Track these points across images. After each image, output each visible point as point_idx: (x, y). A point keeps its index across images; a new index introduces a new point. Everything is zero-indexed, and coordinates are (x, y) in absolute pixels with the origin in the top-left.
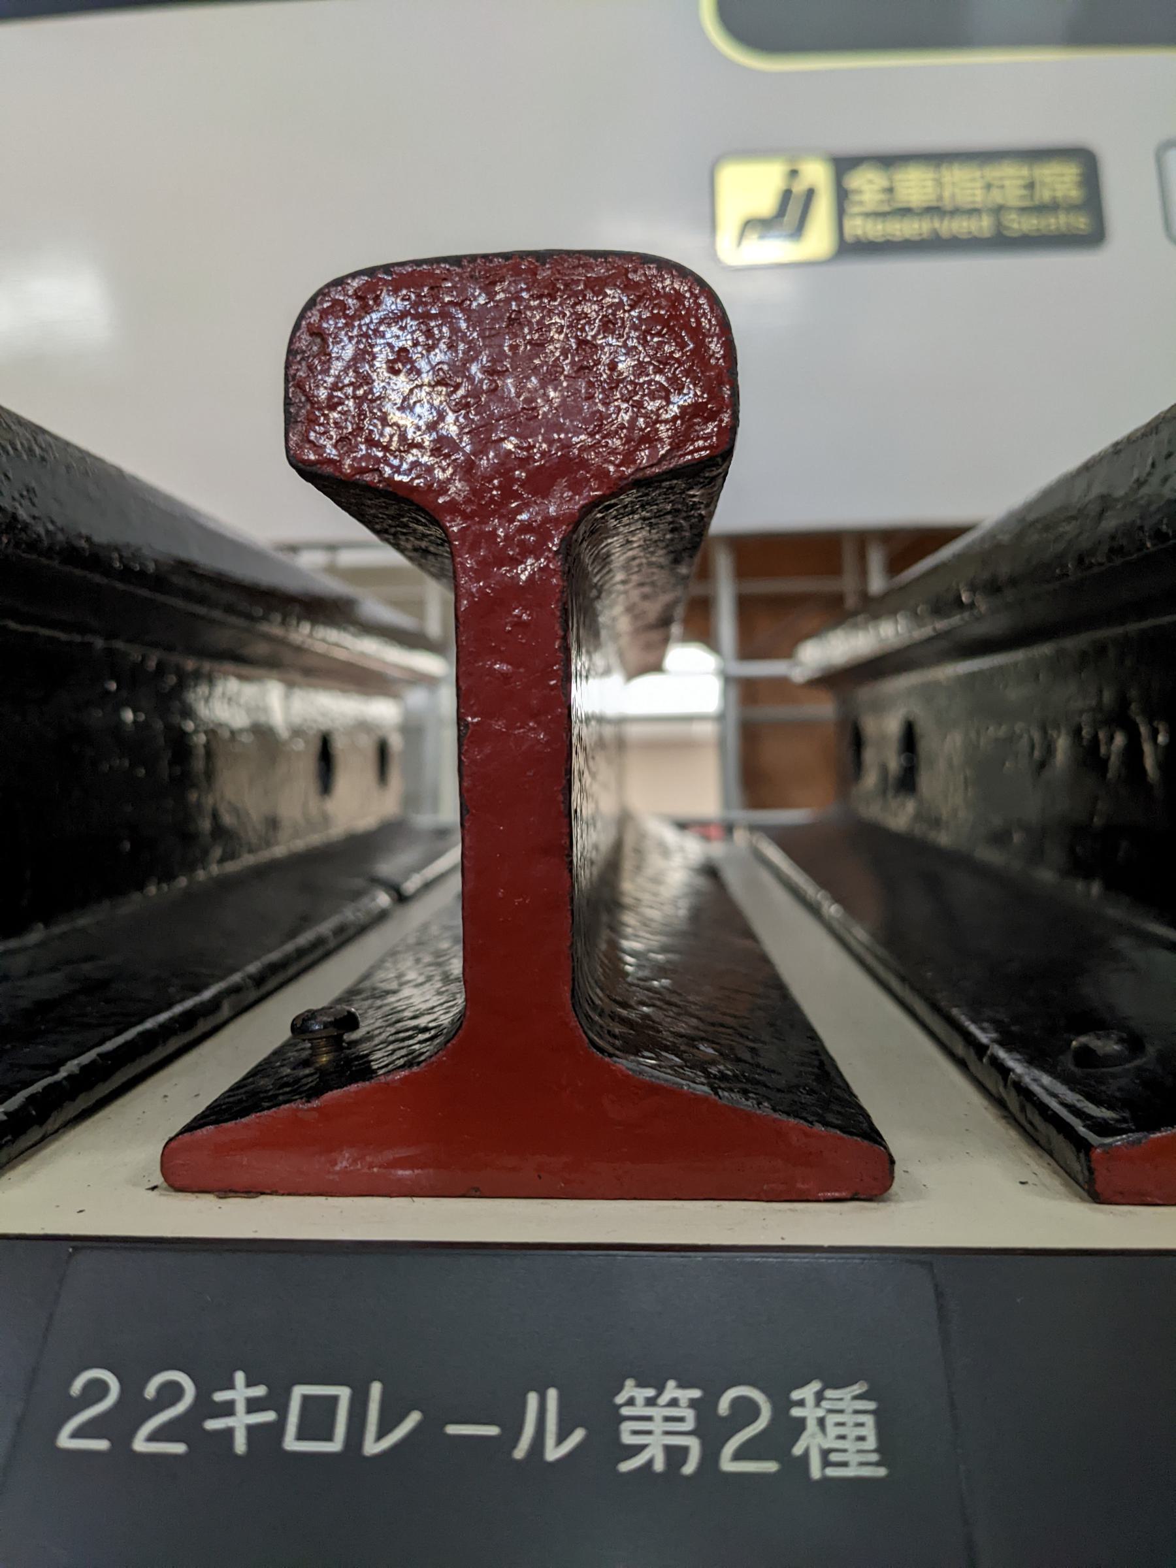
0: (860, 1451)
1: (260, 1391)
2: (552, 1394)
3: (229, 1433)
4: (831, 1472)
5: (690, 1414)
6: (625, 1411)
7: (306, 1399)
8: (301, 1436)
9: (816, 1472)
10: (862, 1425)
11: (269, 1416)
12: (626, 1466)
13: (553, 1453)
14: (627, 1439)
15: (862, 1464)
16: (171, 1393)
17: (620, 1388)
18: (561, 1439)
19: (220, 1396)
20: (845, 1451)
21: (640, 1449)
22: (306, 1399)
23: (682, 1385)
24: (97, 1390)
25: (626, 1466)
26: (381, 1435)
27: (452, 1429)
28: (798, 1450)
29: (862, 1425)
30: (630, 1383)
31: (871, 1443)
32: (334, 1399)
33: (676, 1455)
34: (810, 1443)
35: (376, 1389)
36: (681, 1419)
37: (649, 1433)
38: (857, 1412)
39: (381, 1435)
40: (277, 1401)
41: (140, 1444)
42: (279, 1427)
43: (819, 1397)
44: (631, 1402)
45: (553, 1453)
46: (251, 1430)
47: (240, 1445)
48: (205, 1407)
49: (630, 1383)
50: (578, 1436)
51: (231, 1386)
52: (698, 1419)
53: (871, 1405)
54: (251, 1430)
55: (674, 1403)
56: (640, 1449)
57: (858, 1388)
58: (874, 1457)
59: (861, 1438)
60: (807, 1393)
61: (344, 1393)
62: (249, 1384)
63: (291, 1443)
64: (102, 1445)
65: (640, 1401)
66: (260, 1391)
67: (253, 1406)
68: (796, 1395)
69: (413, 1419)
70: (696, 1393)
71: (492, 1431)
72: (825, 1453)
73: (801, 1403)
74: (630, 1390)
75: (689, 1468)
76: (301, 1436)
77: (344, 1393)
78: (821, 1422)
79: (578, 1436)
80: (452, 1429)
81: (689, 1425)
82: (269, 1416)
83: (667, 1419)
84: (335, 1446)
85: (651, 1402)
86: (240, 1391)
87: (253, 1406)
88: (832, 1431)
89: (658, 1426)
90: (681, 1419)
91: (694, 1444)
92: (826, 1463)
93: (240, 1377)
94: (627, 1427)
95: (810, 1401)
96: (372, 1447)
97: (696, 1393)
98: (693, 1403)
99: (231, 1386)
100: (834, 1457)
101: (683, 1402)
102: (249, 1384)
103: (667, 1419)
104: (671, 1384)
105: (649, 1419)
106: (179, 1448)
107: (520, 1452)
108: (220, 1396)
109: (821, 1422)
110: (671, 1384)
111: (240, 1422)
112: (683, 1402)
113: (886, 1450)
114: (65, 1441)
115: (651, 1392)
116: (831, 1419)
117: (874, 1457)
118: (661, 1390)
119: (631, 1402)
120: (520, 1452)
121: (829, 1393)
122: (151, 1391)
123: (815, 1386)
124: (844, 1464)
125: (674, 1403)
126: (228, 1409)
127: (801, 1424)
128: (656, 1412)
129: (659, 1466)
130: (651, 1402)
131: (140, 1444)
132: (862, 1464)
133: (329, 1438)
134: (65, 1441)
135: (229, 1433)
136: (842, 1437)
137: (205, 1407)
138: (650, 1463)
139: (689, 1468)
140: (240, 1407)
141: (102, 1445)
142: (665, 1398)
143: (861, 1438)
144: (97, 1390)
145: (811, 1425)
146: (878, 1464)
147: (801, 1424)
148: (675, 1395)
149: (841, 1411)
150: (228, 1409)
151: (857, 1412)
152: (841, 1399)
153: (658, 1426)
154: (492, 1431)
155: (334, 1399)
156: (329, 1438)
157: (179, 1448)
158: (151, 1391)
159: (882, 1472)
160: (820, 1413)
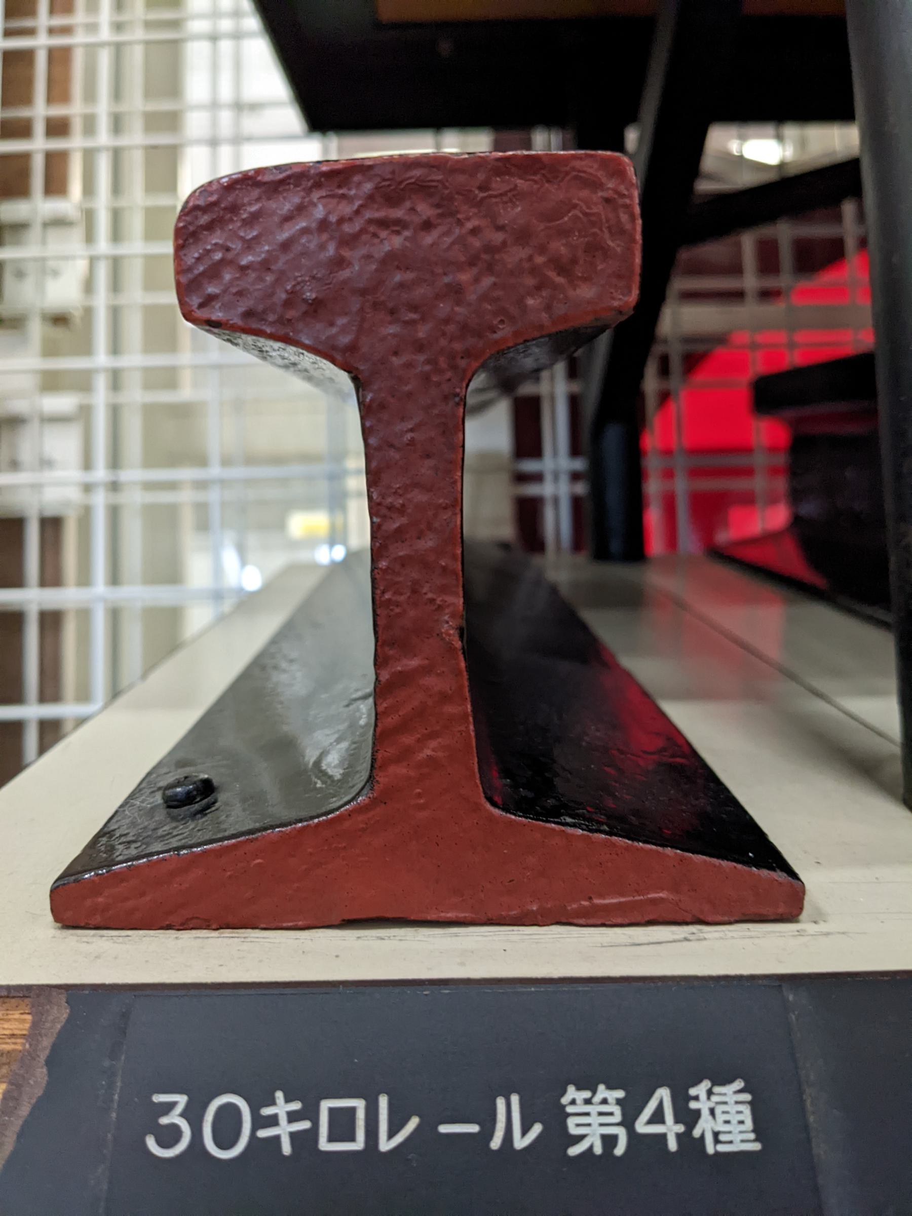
0: (741, 1132)
1: (296, 1106)
2: (515, 1099)
3: (277, 1138)
4: (721, 1148)
5: (617, 1110)
6: (570, 1109)
7: (332, 1111)
8: (331, 1139)
9: (710, 1149)
11: (305, 1125)
12: (574, 1151)
13: (520, 1143)
14: (573, 1130)
15: (743, 1141)
17: (564, 1092)
18: (524, 1132)
19: (267, 1111)
20: (730, 1132)
21: (582, 1137)
23: (610, 1087)
25: (574, 1151)
26: (391, 1135)
27: (444, 1129)
28: (697, 1133)
30: (571, 1090)
31: (749, 1125)
32: (353, 1110)
33: (609, 1141)
34: (704, 1126)
35: (383, 1102)
36: (611, 1114)
37: (589, 1125)
38: (737, 1103)
39: (391, 1135)
40: (310, 1112)
42: (314, 1132)
43: (710, 1093)
44: (573, 1102)
45: (520, 1143)
46: (293, 1136)
47: (286, 1148)
49: (571, 1090)
50: (537, 1129)
51: (273, 1103)
52: (624, 1114)
53: (747, 1097)
54: (293, 1136)
55: (605, 1101)
56: (582, 1137)
57: (739, 1084)
58: (752, 1136)
59: (741, 1122)
60: (700, 1090)
61: (359, 1105)
62: (287, 1100)
63: (324, 1145)
65: (578, 1101)
66: (296, 1106)
67: (293, 1117)
68: (693, 1092)
69: (413, 1123)
70: (620, 1094)
71: (474, 1128)
72: (716, 1135)
73: (696, 1098)
74: (572, 1092)
75: (620, 1150)
76: (331, 1139)
77: (359, 1105)
78: (712, 1112)
79: (537, 1129)
80: (444, 1129)
81: (617, 1118)
82: (305, 1125)
83: (601, 1114)
84: (359, 1145)
85: (588, 1102)
86: (281, 1107)
87: (293, 1117)
88: (721, 1118)
89: (594, 1120)
90: (611, 1114)
91: (621, 1133)
92: (717, 1141)
93: (279, 1095)
94: (571, 1122)
95: (703, 1096)
96: (385, 1145)
97: (620, 1094)
98: (619, 1102)
99: (273, 1103)
100: (722, 1137)
101: (610, 1100)
102: (287, 1100)
103: (601, 1114)
104: (601, 1087)
105: (587, 1114)
107: (496, 1143)
108: (267, 1111)
109: (712, 1112)
110: (601, 1087)
111: (284, 1130)
113: (759, 1131)
115: (587, 1094)
116: (719, 1110)
118: (594, 1092)
119: (573, 1102)
120: (496, 1143)
121: (717, 1089)
123: (705, 1085)
124: (731, 1142)
125: (605, 1101)
126: (273, 1121)
127: (697, 1114)
128: (592, 1109)
129: (598, 1150)
130: (588, 1102)
132: (743, 1141)
133: (352, 1138)
135: (277, 1138)
136: (727, 1122)
138: (591, 1148)
139: (620, 1150)
140: (283, 1119)
143: (741, 1122)
145: (705, 1113)
146: (755, 1140)
147: (697, 1114)
149: (725, 1103)
150: (273, 1121)
151: (737, 1103)
152: (725, 1094)
153: (594, 1120)
154: (474, 1128)
155: (353, 1110)
156: (352, 1138)
159: (757, 1146)
160: (711, 1105)
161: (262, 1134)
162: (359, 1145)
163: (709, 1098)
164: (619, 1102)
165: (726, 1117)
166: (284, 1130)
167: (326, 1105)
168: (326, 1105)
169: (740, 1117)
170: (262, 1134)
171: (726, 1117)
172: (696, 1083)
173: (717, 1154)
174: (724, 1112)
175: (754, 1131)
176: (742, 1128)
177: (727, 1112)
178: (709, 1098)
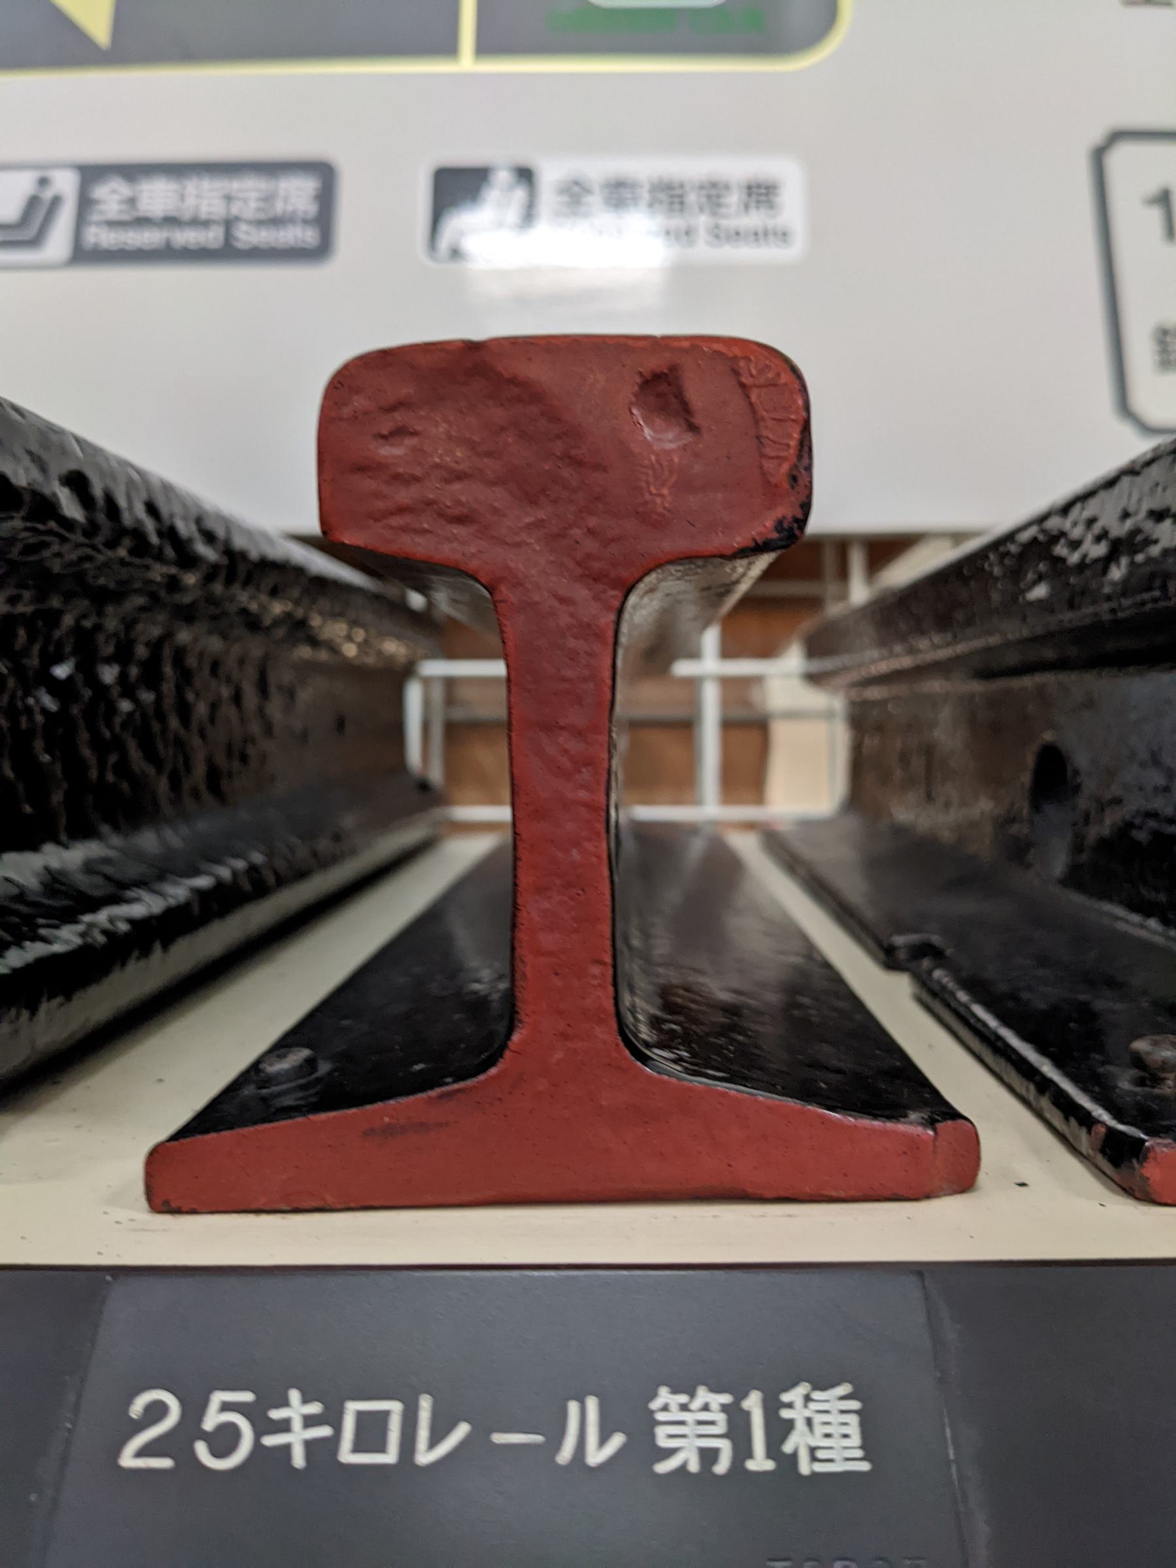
1: (315, 1408)
3: (287, 1449)
4: (819, 1468)
8: (357, 1448)
11: (325, 1431)
19: (276, 1414)
31: (856, 1440)
32: (386, 1414)
38: (843, 1412)
40: (333, 1417)
42: (334, 1442)
43: (808, 1399)
46: (309, 1445)
47: (298, 1459)
51: (285, 1403)
54: (309, 1445)
57: (844, 1389)
58: (859, 1453)
59: (846, 1436)
60: (794, 1395)
62: (305, 1400)
63: (347, 1455)
66: (315, 1408)
67: (310, 1421)
68: (786, 1397)
73: (790, 1405)
76: (357, 1448)
78: (809, 1422)
82: (325, 1431)
84: (390, 1457)
86: (296, 1408)
87: (310, 1421)
88: (819, 1430)
92: (814, 1459)
93: (294, 1396)
99: (285, 1403)
102: (305, 1400)
108: (276, 1414)
109: (809, 1422)
111: (296, 1439)
113: (869, 1447)
116: (818, 1419)
121: (816, 1395)
123: (802, 1389)
126: (284, 1426)
135: (287, 1449)
136: (828, 1436)
140: (297, 1424)
143: (846, 1436)
145: (800, 1425)
149: (827, 1412)
150: (284, 1426)
151: (843, 1412)
159: (865, 1466)
160: (807, 1413)
161: (270, 1441)
162: (390, 1457)
163: (806, 1406)
165: (828, 1429)
166: (296, 1439)
167: (353, 1407)
169: (845, 1430)
170: (270, 1441)
173: (815, 1475)
175: (863, 1447)
176: (846, 1442)
178: (806, 1406)
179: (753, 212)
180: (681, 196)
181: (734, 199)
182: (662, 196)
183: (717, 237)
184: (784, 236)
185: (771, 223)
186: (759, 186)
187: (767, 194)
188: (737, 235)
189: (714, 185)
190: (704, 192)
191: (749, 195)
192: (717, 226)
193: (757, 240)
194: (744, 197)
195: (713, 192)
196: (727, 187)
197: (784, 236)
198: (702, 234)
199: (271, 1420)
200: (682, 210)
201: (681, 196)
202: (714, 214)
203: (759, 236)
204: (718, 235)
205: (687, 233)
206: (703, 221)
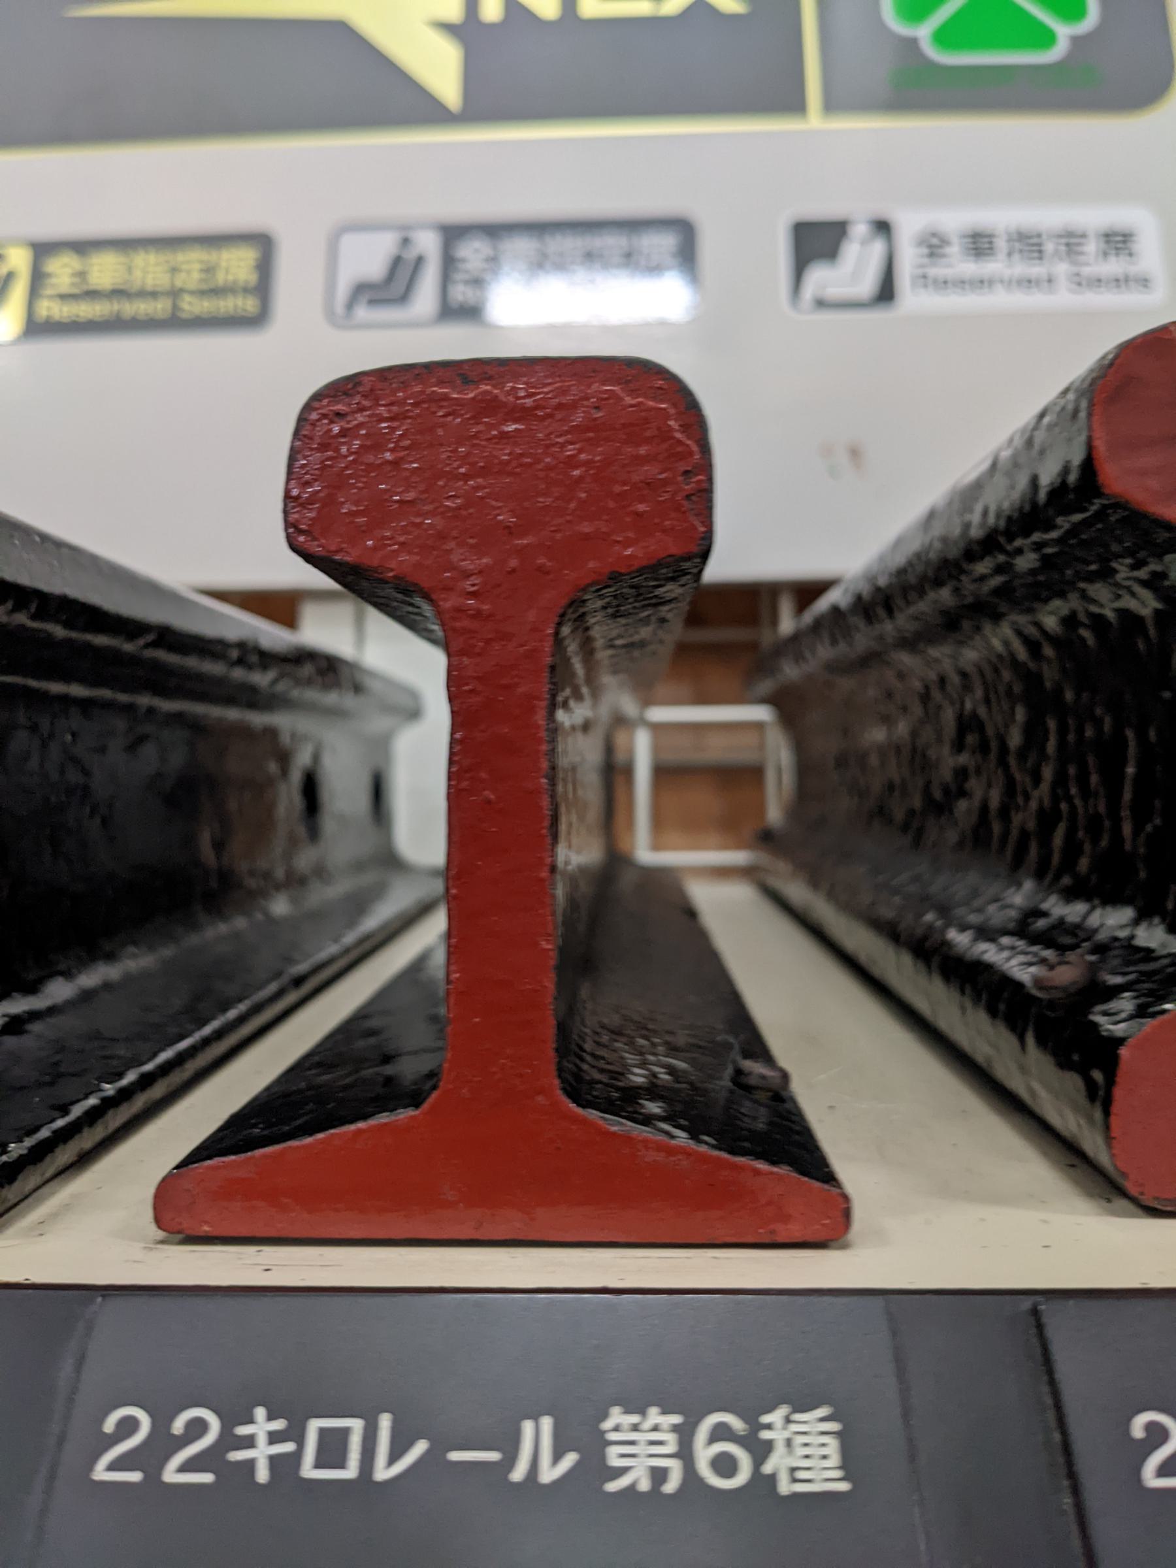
1: (279, 1425)
2: (547, 1423)
3: (250, 1464)
6: (613, 1436)
7: (323, 1432)
8: (318, 1465)
9: (785, 1487)
10: (823, 1445)
11: (289, 1447)
14: (615, 1462)
16: (197, 1428)
19: (243, 1430)
21: (624, 1471)
22: (323, 1432)
23: (665, 1412)
24: (128, 1427)
27: (455, 1456)
28: (767, 1468)
29: (823, 1445)
31: (834, 1460)
33: (659, 1475)
35: (385, 1422)
40: (296, 1433)
41: (171, 1474)
42: (297, 1456)
43: (788, 1420)
44: (617, 1429)
46: (273, 1460)
47: (262, 1475)
48: (229, 1441)
51: (251, 1421)
54: (273, 1460)
55: (655, 1428)
56: (624, 1471)
58: (837, 1474)
59: (825, 1457)
60: (775, 1417)
61: (356, 1425)
62: (271, 1417)
64: (135, 1477)
66: (279, 1425)
67: (274, 1438)
68: (766, 1419)
69: (420, 1448)
70: (676, 1419)
71: (493, 1456)
73: (769, 1427)
74: (617, 1417)
75: (671, 1486)
76: (318, 1465)
77: (356, 1425)
81: (671, 1448)
82: (289, 1447)
83: (653, 1443)
85: (635, 1428)
86: (261, 1425)
87: (274, 1438)
91: (675, 1467)
97: (676, 1419)
98: (675, 1428)
99: (251, 1421)
100: (801, 1475)
102: (271, 1417)
103: (653, 1443)
105: (632, 1443)
106: (207, 1478)
108: (243, 1430)
109: (789, 1443)
111: (261, 1454)
112: (665, 1426)
113: (848, 1466)
114: (101, 1473)
115: (634, 1419)
117: (837, 1474)
119: (617, 1429)
121: (798, 1417)
122: (179, 1425)
125: (655, 1428)
126: (249, 1442)
127: (769, 1446)
130: (635, 1428)
131: (171, 1474)
134: (101, 1473)
135: (250, 1464)
137: (229, 1441)
139: (671, 1486)
140: (262, 1440)
141: (135, 1477)
142: (647, 1424)
143: (825, 1457)
144: (128, 1427)
147: (769, 1446)
148: (657, 1421)
150: (249, 1442)
154: (493, 1456)
155: (345, 1432)
156: (341, 1465)
157: (207, 1478)
158: (179, 1425)
159: (844, 1486)
160: (786, 1434)
164: (675, 1428)
165: (807, 1451)
166: (261, 1454)
168: (314, 1426)
169: (824, 1451)
171: (807, 1451)
172: (770, 1410)
174: (806, 1445)
177: (806, 1445)
179: (1112, 259)
180: (1040, 245)
181: (1091, 247)
182: (1017, 245)
183: (1079, 284)
184: (1144, 282)
185: (1133, 270)
186: (1116, 234)
187: (1124, 242)
188: (1097, 282)
189: (1070, 234)
190: (1063, 241)
191: (1107, 242)
192: (1078, 275)
193: (1118, 287)
194: (1102, 245)
195: (1071, 241)
196: (1084, 236)
197: (1144, 282)
198: (1063, 283)
199: (237, 1436)
200: (1041, 258)
201: (1040, 245)
202: (1074, 263)
203: (1120, 282)
204: (1080, 282)
205: (1050, 281)
206: (1062, 269)
